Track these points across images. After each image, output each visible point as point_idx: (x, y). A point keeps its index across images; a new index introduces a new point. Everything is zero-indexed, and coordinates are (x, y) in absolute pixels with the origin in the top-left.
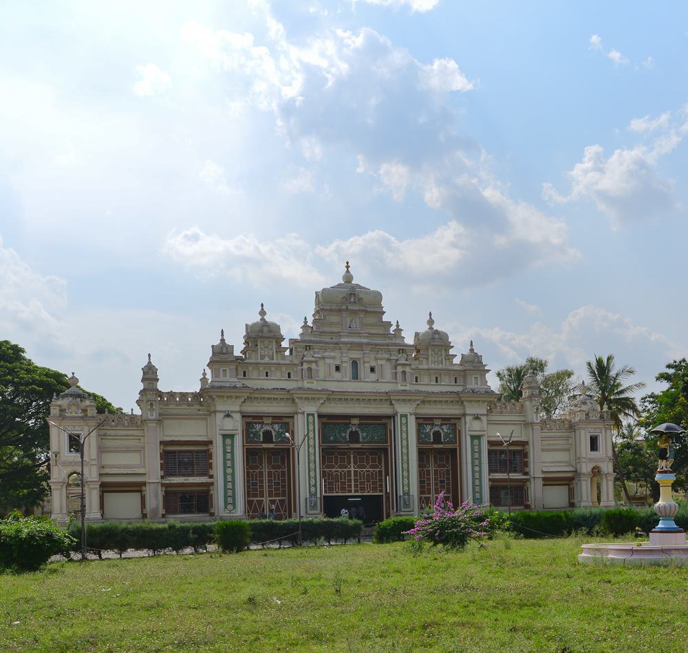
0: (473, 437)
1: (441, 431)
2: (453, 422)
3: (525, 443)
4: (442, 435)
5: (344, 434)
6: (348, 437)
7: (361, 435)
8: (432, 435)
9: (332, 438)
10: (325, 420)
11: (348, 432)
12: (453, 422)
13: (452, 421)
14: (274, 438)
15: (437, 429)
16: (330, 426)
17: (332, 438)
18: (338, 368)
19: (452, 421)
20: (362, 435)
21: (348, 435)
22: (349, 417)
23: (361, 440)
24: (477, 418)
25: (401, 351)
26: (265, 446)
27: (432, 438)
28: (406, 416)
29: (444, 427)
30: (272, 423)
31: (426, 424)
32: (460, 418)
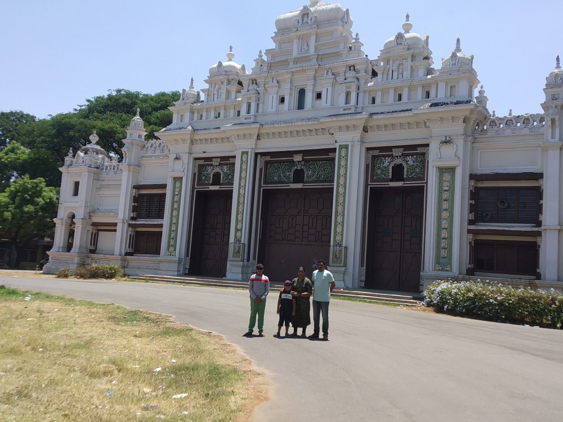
0: (442, 170)
1: (404, 164)
2: (418, 151)
3: (539, 176)
4: (405, 169)
5: (288, 174)
6: (292, 176)
7: (306, 173)
8: (391, 170)
9: (276, 178)
10: (268, 158)
11: (293, 171)
12: (418, 151)
13: (420, 150)
14: (222, 180)
15: (398, 161)
16: (276, 164)
17: (276, 178)
18: (282, 100)
19: (420, 150)
20: (308, 173)
21: (292, 174)
22: (291, 153)
23: (305, 179)
24: (447, 142)
25: (352, 68)
26: (212, 188)
27: (390, 174)
28: (346, 147)
29: (409, 159)
30: (220, 164)
31: (385, 156)
32: (427, 145)
